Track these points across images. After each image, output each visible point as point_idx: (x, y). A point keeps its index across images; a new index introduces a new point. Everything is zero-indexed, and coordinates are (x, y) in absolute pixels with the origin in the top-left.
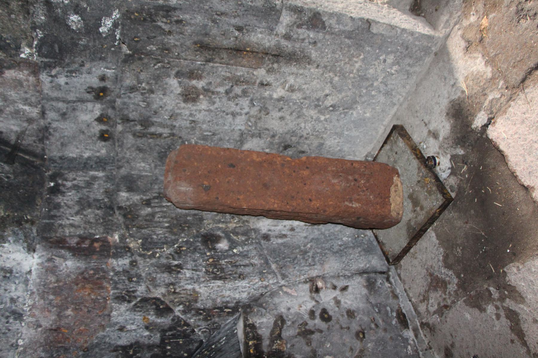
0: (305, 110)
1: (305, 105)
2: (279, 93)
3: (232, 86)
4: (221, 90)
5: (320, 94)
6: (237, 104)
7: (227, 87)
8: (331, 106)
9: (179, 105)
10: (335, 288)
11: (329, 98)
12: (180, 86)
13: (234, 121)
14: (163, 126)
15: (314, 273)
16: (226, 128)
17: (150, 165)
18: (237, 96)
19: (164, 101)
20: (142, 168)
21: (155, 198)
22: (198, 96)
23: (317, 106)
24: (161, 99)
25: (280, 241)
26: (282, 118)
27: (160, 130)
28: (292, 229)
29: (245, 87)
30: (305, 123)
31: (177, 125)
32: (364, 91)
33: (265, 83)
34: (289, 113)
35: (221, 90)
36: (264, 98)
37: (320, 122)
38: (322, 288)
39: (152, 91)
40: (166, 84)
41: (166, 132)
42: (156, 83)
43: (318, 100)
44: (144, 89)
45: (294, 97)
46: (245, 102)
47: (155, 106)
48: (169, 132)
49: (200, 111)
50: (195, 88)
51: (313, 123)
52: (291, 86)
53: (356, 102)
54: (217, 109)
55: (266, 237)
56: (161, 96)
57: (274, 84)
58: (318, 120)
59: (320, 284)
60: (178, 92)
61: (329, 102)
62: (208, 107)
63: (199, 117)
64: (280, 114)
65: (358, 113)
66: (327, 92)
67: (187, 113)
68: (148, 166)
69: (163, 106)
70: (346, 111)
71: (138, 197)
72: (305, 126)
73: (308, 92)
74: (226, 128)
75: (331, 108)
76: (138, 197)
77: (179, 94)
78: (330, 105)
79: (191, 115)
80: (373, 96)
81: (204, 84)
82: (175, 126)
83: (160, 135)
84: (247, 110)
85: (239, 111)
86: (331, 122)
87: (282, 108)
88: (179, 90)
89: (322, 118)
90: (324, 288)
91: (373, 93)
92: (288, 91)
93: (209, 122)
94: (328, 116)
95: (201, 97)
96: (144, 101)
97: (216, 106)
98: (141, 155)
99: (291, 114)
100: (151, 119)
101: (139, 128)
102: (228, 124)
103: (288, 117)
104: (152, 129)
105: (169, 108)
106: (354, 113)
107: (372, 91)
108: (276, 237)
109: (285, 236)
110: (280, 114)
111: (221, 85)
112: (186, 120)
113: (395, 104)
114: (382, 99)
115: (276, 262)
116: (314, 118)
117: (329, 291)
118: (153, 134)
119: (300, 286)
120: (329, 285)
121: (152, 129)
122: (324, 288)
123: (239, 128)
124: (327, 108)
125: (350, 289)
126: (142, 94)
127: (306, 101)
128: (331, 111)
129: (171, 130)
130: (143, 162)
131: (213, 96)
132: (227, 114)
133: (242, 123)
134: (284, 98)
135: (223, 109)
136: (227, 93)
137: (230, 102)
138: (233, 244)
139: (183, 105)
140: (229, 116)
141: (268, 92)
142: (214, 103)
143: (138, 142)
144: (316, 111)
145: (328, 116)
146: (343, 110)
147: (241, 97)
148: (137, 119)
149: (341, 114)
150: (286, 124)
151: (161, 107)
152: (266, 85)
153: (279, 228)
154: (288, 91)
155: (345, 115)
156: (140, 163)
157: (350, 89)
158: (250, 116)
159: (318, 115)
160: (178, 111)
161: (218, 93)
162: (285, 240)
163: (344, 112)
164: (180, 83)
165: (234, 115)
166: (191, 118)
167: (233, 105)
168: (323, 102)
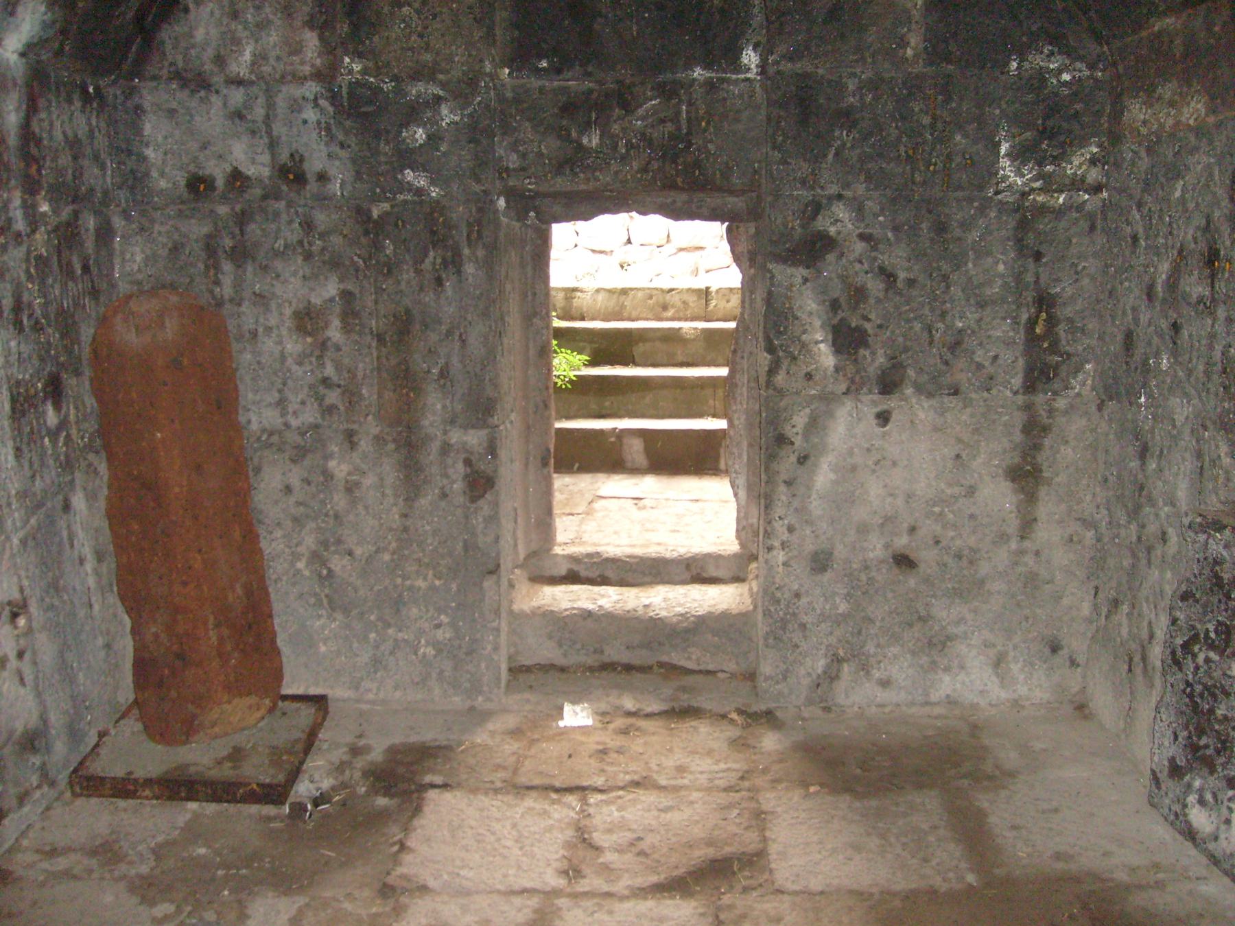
0: (313, 525)
1: (323, 521)
2: (340, 468)
3: (339, 386)
4: (329, 371)
5: (351, 541)
6: (303, 403)
7: (335, 379)
8: (330, 570)
9: (287, 304)
10: (20, 655)
11: (346, 560)
12: (325, 302)
13: (267, 406)
14: (238, 285)
15: (33, 608)
16: (250, 396)
17: (139, 270)
18: (320, 399)
19: (292, 280)
20: (128, 256)
21: (92, 282)
22: (310, 334)
23: (325, 544)
24: (295, 274)
25: (65, 534)
26: (288, 489)
27: (227, 280)
28: (82, 561)
29: (342, 408)
30: (284, 536)
31: (243, 309)
32: (372, 618)
33: (355, 439)
34: (301, 500)
35: (329, 371)
36: (324, 446)
37: (292, 564)
38: (16, 627)
39: (308, 257)
40: (326, 279)
41: (227, 290)
42: (324, 262)
43: (339, 542)
44: (310, 244)
45: (336, 498)
46: (310, 415)
47: (279, 265)
48: (226, 297)
49: (280, 343)
50: (327, 326)
51: (287, 550)
52: (357, 484)
53: (346, 611)
54: (289, 370)
55: (67, 507)
56: (301, 273)
57: (354, 455)
58: (296, 557)
59: (22, 622)
60: (313, 300)
61: (338, 564)
62: (291, 355)
63: (268, 344)
64: (295, 482)
65: (323, 627)
66: (358, 551)
67: (273, 322)
68: (136, 267)
69: (282, 278)
70: (325, 601)
71: (90, 251)
72: (277, 539)
73: (351, 517)
74: (250, 396)
75: (325, 572)
76: (90, 251)
77: (309, 302)
78: (332, 566)
79: (268, 330)
80: (366, 638)
81: (334, 340)
82: (240, 305)
83: (217, 283)
84: (294, 423)
85: (290, 410)
86: (294, 584)
87: (309, 483)
88: (316, 300)
89: (300, 565)
90: (16, 632)
91: (373, 635)
92: (347, 482)
93: (259, 363)
94: (307, 573)
95: (309, 340)
96: (286, 246)
97: (295, 368)
98: (164, 252)
99: (299, 504)
100: (250, 261)
101: (228, 243)
102: (258, 398)
103: (292, 500)
104: (227, 267)
105: (279, 289)
106: (322, 621)
107: (376, 632)
108: (69, 527)
109: (72, 546)
110: (295, 482)
111: (338, 367)
112: (257, 321)
113: (357, 688)
114: (365, 657)
115: (39, 528)
116: (299, 549)
117: (14, 644)
118: (217, 267)
119: (15, 579)
120: (22, 642)
121: (227, 267)
122: (16, 632)
123: (254, 419)
124: (324, 564)
125: (22, 691)
126: (301, 243)
127: (332, 521)
128: (320, 576)
129: (231, 300)
130: (146, 259)
131: (314, 359)
132: (280, 391)
133: (264, 421)
134: (332, 478)
135: (290, 382)
136: (325, 381)
137: (306, 390)
138: (54, 434)
139: (288, 312)
140: (277, 395)
141: (336, 449)
142: (300, 364)
143: (195, 245)
144: (313, 547)
145: (307, 573)
146: (327, 596)
147: (320, 405)
148: (246, 237)
149: (316, 594)
150: (276, 502)
151: (278, 276)
152: (351, 442)
153: (80, 531)
154: (347, 482)
155: (314, 605)
156: (143, 252)
157: (371, 589)
158: (280, 433)
159: (307, 554)
160: (273, 305)
161: (323, 365)
162: (67, 546)
163: (321, 600)
164: (332, 300)
165: (281, 403)
166: (261, 330)
167: (300, 397)
168: (335, 552)
